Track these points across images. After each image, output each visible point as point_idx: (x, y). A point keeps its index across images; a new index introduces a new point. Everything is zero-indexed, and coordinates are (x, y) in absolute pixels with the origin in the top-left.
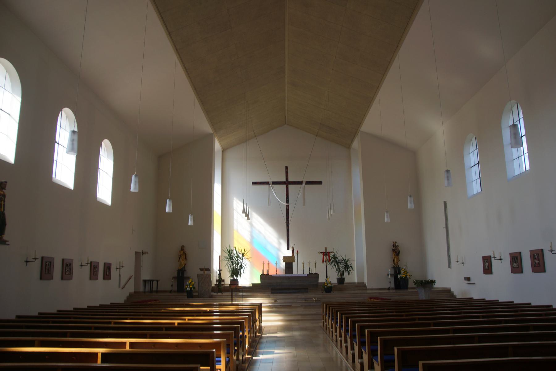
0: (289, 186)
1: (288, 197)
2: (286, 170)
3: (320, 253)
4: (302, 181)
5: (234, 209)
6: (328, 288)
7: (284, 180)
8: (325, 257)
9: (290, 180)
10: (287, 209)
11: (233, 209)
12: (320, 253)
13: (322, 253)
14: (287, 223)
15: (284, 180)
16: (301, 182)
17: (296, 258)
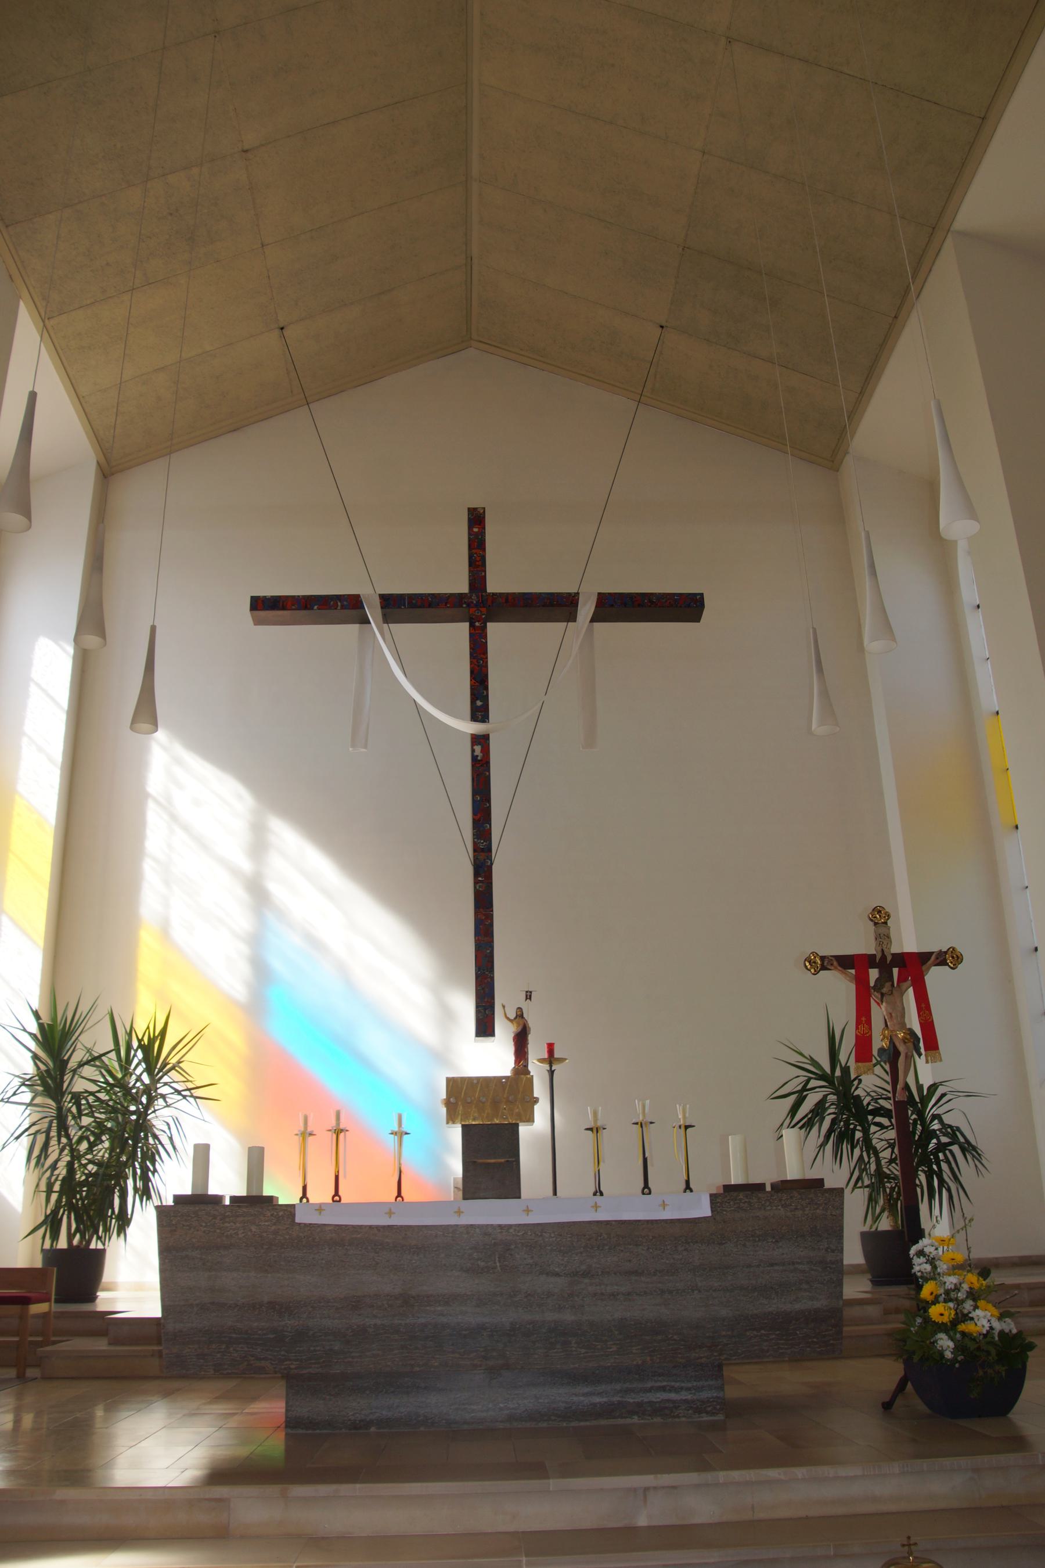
0: (492, 628)
1: (486, 688)
2: (470, 528)
3: (823, 963)
4: (573, 590)
5: (146, 796)
6: (967, 1345)
7: (460, 585)
8: (878, 1012)
9: (495, 585)
10: (474, 759)
11: (142, 796)
12: (823, 963)
13: (844, 962)
14: (475, 851)
15: (460, 585)
16: (570, 594)
17: (540, 1089)
